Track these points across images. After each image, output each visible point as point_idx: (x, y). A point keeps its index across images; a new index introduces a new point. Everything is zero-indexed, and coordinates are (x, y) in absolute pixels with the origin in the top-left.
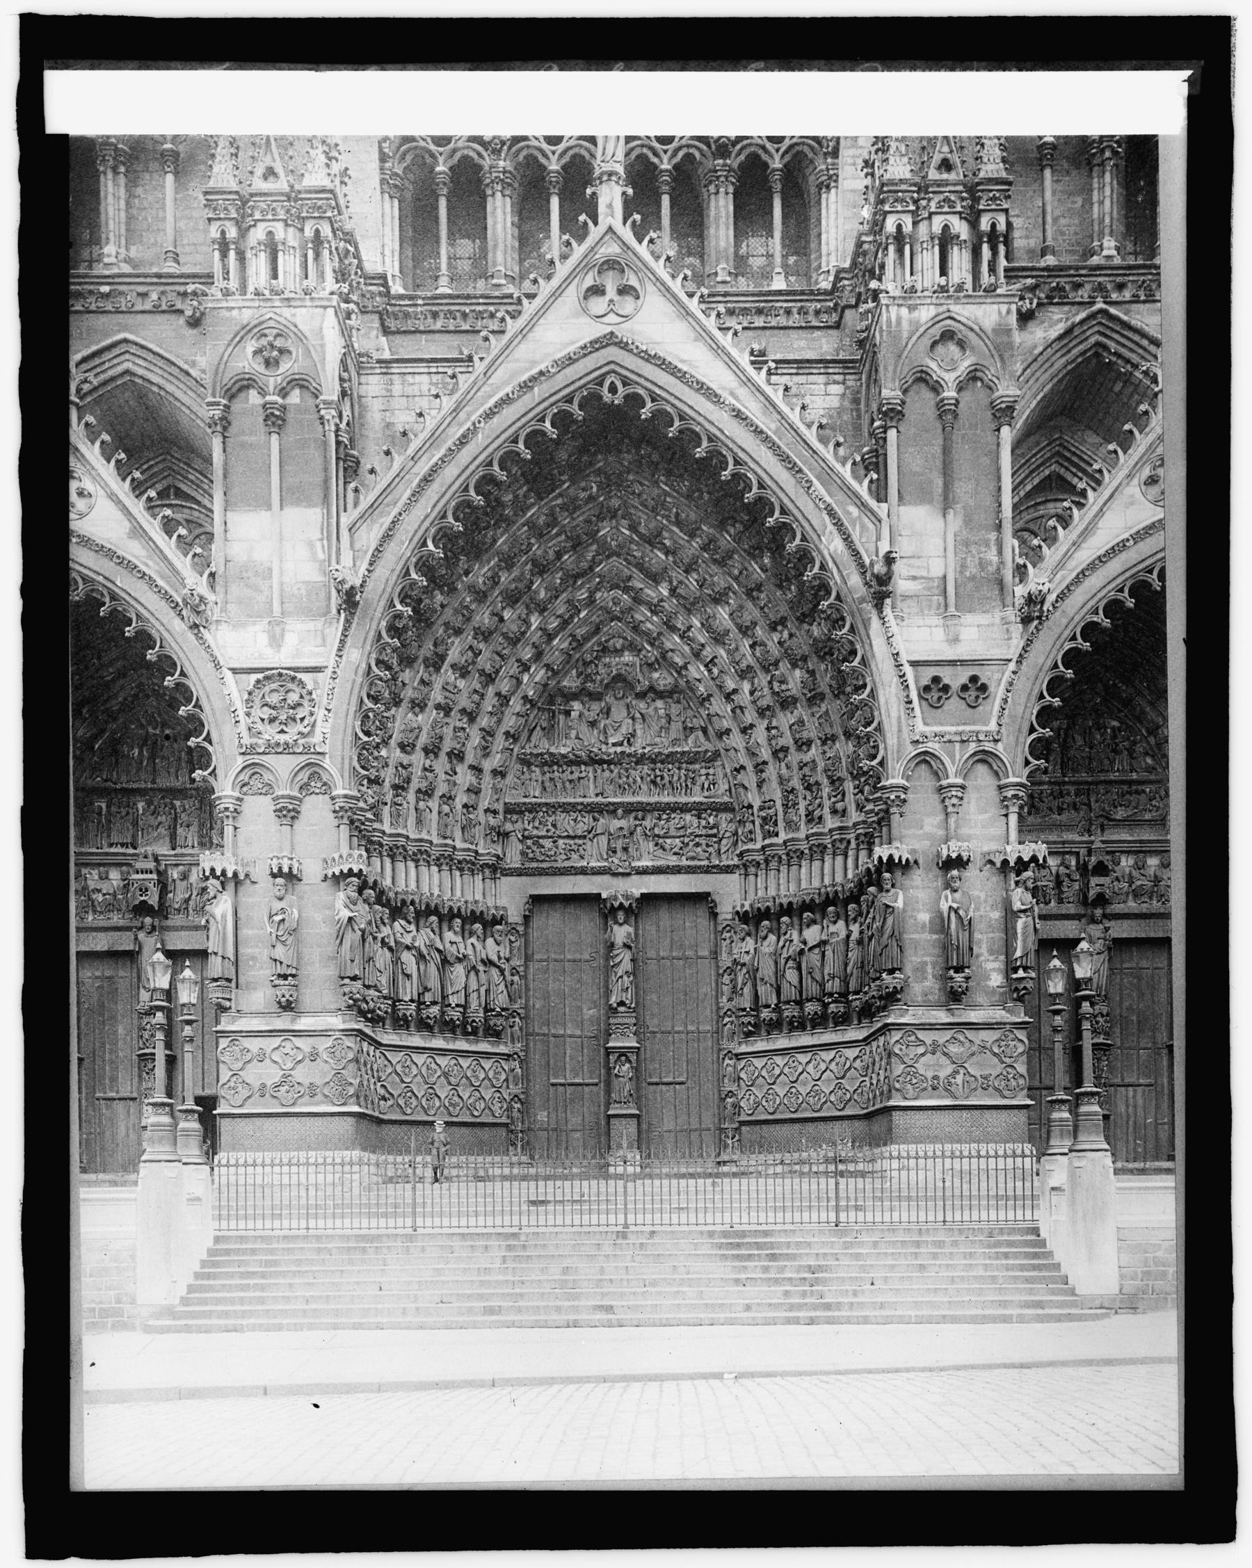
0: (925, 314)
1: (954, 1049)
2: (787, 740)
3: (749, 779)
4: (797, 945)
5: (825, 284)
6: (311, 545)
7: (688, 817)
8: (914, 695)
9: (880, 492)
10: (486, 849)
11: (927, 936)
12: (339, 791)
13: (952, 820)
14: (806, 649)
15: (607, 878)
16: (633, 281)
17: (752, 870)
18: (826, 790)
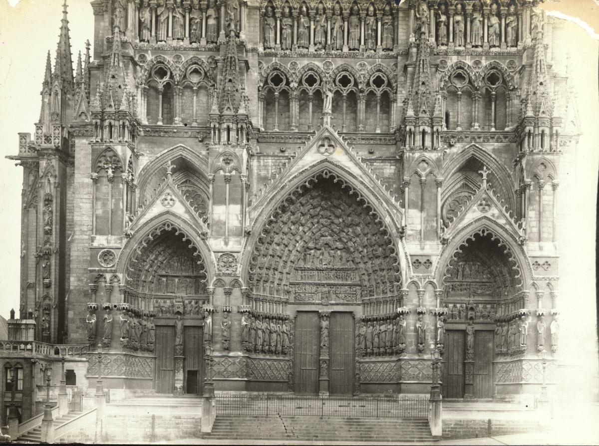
0: (417, 155)
1: (419, 366)
2: (377, 268)
3: (366, 277)
4: (378, 331)
5: (392, 131)
6: (237, 215)
7: (347, 287)
8: (411, 265)
9: (403, 206)
10: (283, 297)
11: (413, 333)
12: (243, 288)
13: (421, 301)
14: (383, 243)
15: (320, 306)
16: (333, 143)
17: (366, 305)
18: (388, 284)
